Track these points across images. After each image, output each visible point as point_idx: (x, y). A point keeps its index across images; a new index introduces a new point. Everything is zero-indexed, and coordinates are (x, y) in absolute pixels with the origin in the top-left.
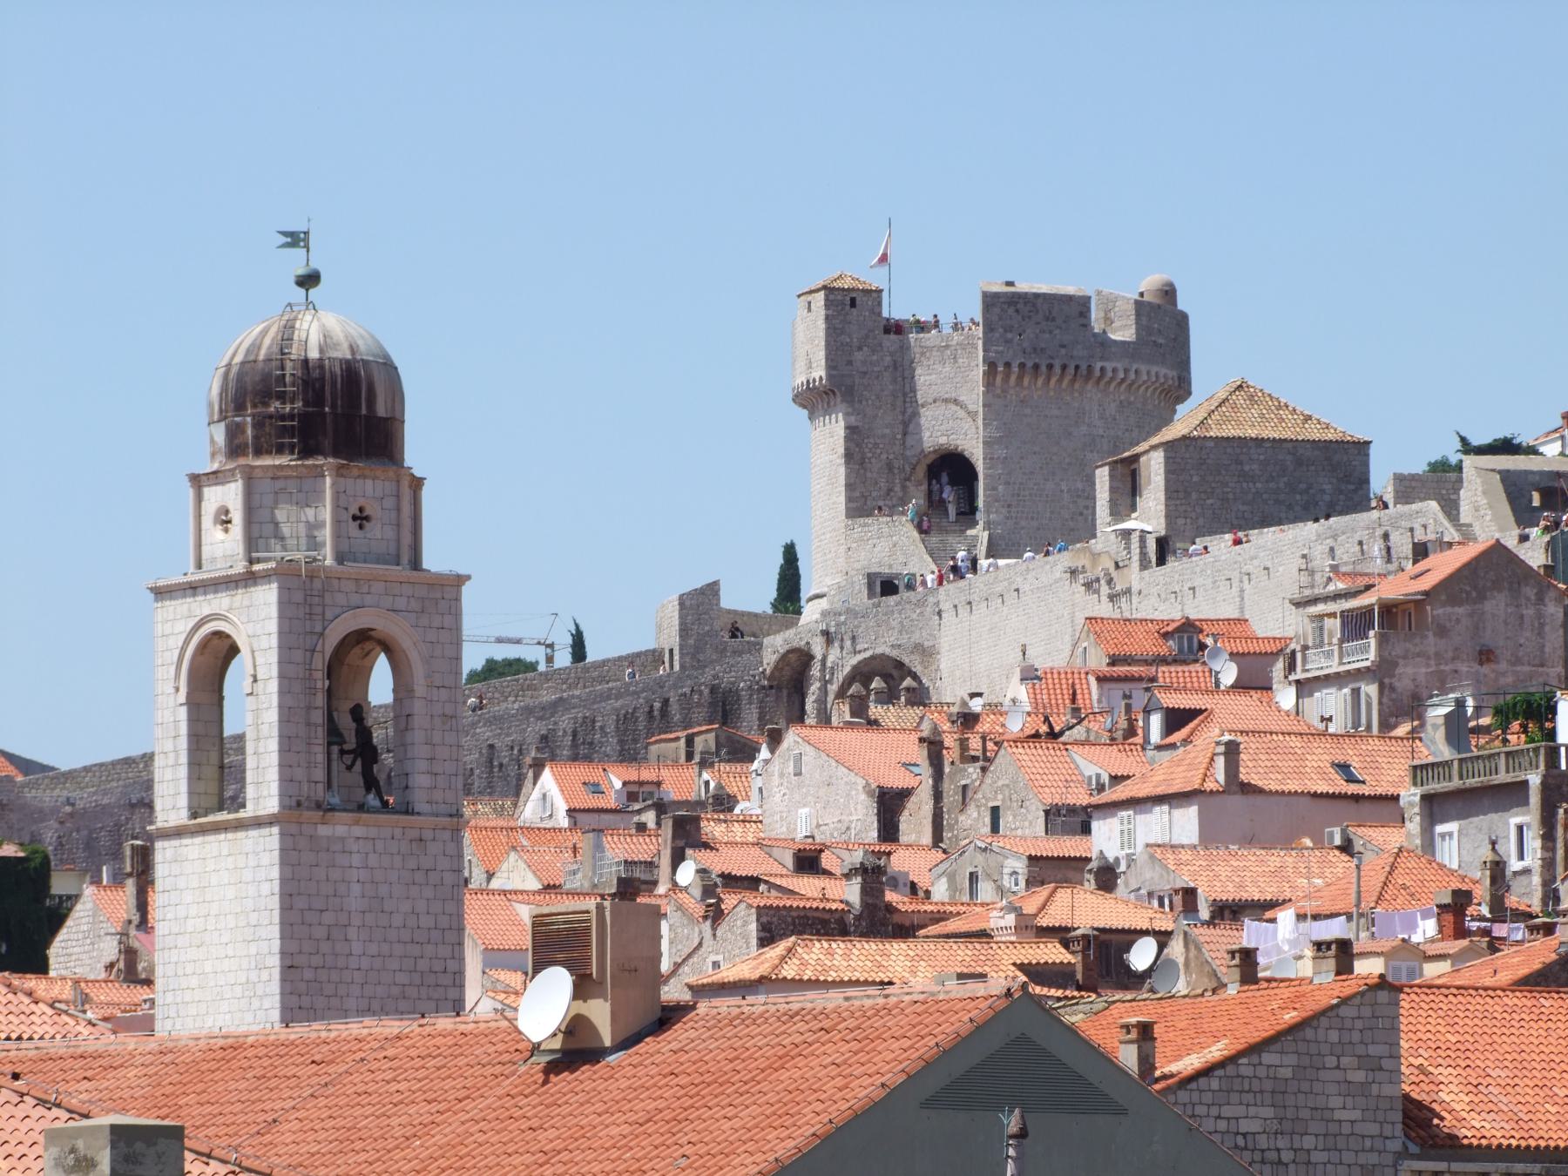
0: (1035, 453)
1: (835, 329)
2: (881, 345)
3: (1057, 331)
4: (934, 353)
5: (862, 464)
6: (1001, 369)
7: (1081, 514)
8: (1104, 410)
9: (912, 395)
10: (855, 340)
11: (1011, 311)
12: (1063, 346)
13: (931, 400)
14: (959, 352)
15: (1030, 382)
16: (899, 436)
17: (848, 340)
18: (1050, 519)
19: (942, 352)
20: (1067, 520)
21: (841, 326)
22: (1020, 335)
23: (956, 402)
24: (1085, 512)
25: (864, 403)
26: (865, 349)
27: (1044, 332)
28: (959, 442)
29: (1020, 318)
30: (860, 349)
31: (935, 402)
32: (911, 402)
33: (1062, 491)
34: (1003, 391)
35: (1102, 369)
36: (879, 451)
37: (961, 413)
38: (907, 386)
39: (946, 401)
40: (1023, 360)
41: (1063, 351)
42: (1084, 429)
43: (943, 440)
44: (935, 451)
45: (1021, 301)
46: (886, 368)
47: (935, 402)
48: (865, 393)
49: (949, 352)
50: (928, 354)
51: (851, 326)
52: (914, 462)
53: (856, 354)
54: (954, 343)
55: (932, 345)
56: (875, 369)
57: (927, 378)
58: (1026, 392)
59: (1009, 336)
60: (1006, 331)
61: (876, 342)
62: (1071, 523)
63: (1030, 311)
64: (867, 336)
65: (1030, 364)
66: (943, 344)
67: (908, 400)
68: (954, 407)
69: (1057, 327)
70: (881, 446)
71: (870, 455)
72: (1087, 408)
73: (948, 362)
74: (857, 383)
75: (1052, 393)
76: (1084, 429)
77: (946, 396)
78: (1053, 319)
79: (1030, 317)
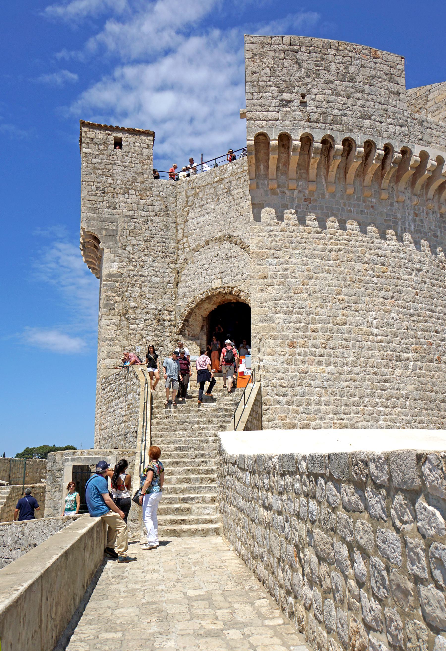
0: (328, 272)
1: (95, 168)
2: (150, 189)
3: (359, 95)
4: (207, 192)
5: (124, 315)
6: (274, 143)
8: (422, 221)
9: (185, 240)
10: (119, 182)
13: (204, 243)
14: (234, 183)
15: (318, 175)
16: (170, 286)
17: (110, 181)
19: (215, 188)
21: (102, 166)
22: (303, 96)
23: (230, 238)
25: (129, 248)
26: (131, 192)
27: (338, 95)
28: (233, 284)
29: (302, 73)
30: (126, 192)
31: (207, 243)
32: (184, 248)
34: (279, 186)
36: (145, 301)
37: (237, 250)
38: (180, 232)
39: (219, 239)
40: (307, 131)
41: (367, 122)
43: (216, 284)
44: (209, 298)
45: (303, 49)
46: (157, 214)
47: (207, 243)
48: (129, 238)
49: (222, 187)
50: (201, 195)
51: (115, 167)
52: (186, 313)
53: (120, 196)
54: (228, 174)
55: (205, 183)
56: (143, 213)
57: (200, 219)
58: (312, 187)
60: (281, 91)
61: (145, 186)
63: (317, 65)
64: (134, 180)
66: (216, 179)
67: (180, 247)
68: (228, 245)
69: (357, 91)
70: (149, 296)
71: (135, 305)
72: (399, 216)
73: (221, 197)
74: (120, 227)
75: (350, 191)
77: (220, 234)
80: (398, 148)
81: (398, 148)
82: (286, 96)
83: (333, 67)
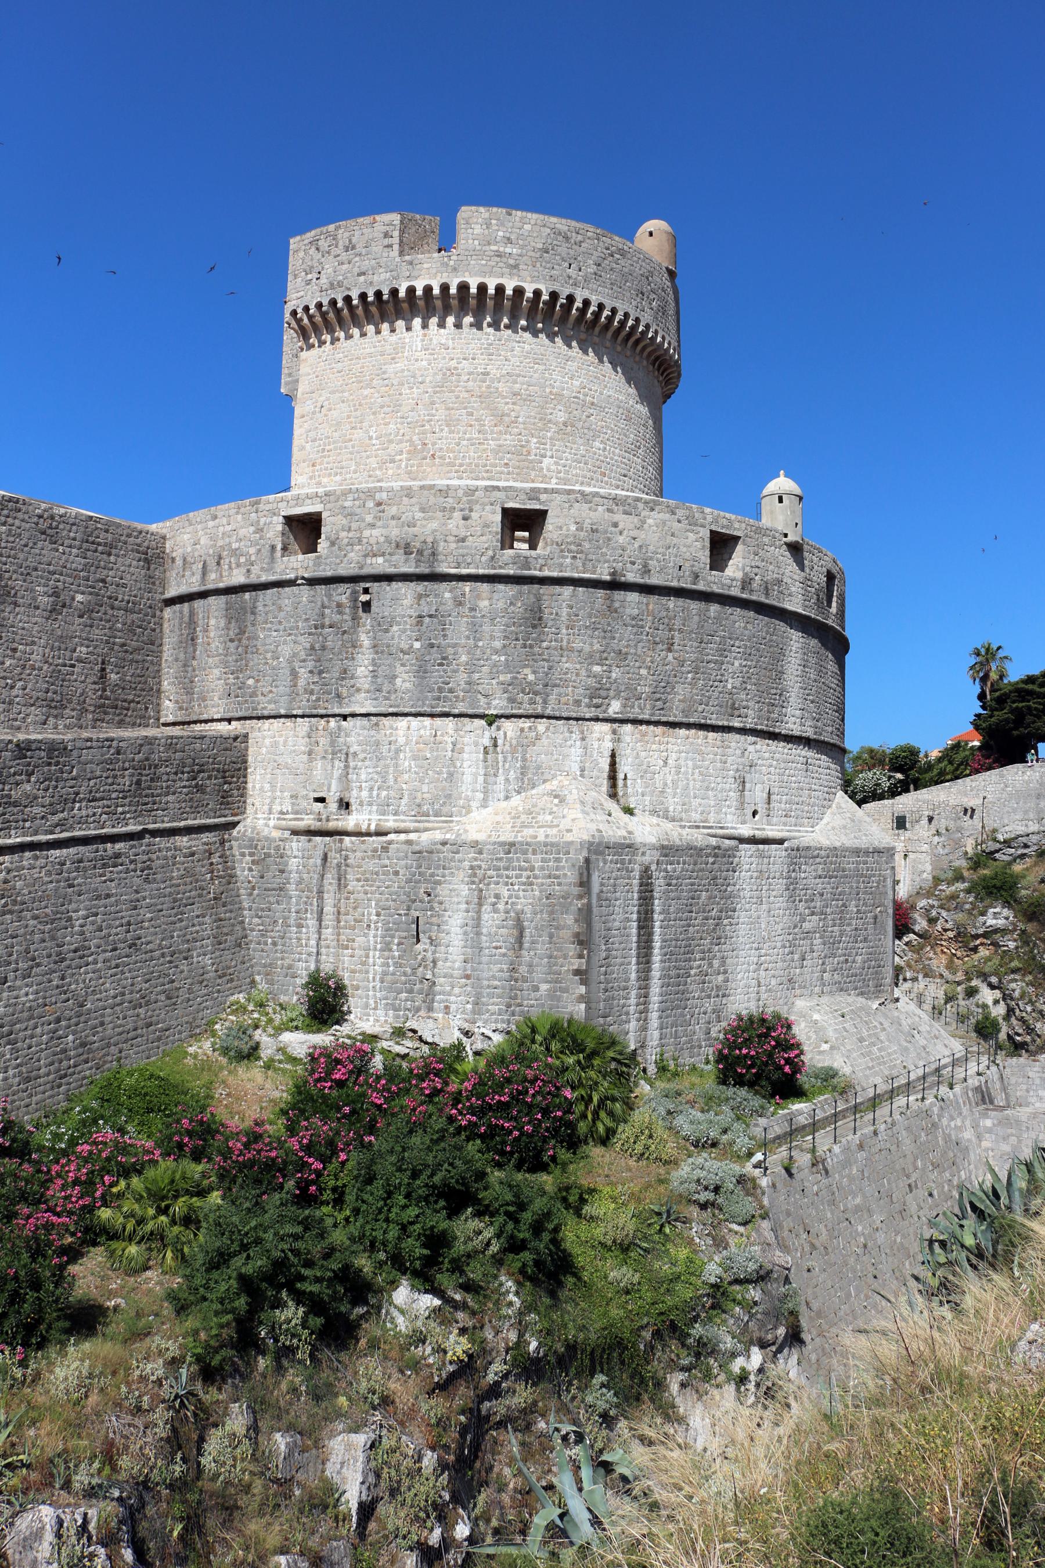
7: (393, 461)
11: (313, 250)
12: (359, 275)
18: (355, 472)
20: (374, 470)
24: (398, 458)
33: (370, 438)
35: (411, 290)
41: (362, 278)
42: (400, 366)
59: (309, 277)
62: (378, 473)
65: (325, 302)
76: (400, 366)
78: (354, 248)
79: (328, 253)
80: (386, 291)
81: (386, 291)
82: (309, 277)
83: (341, 243)
